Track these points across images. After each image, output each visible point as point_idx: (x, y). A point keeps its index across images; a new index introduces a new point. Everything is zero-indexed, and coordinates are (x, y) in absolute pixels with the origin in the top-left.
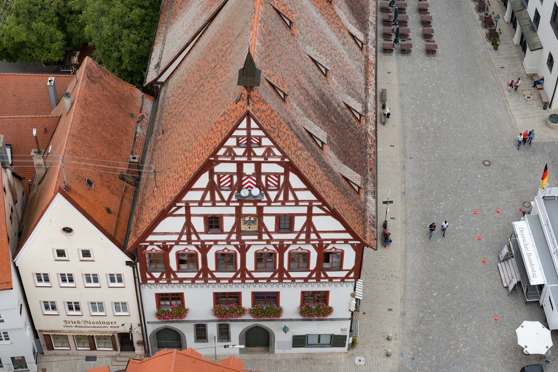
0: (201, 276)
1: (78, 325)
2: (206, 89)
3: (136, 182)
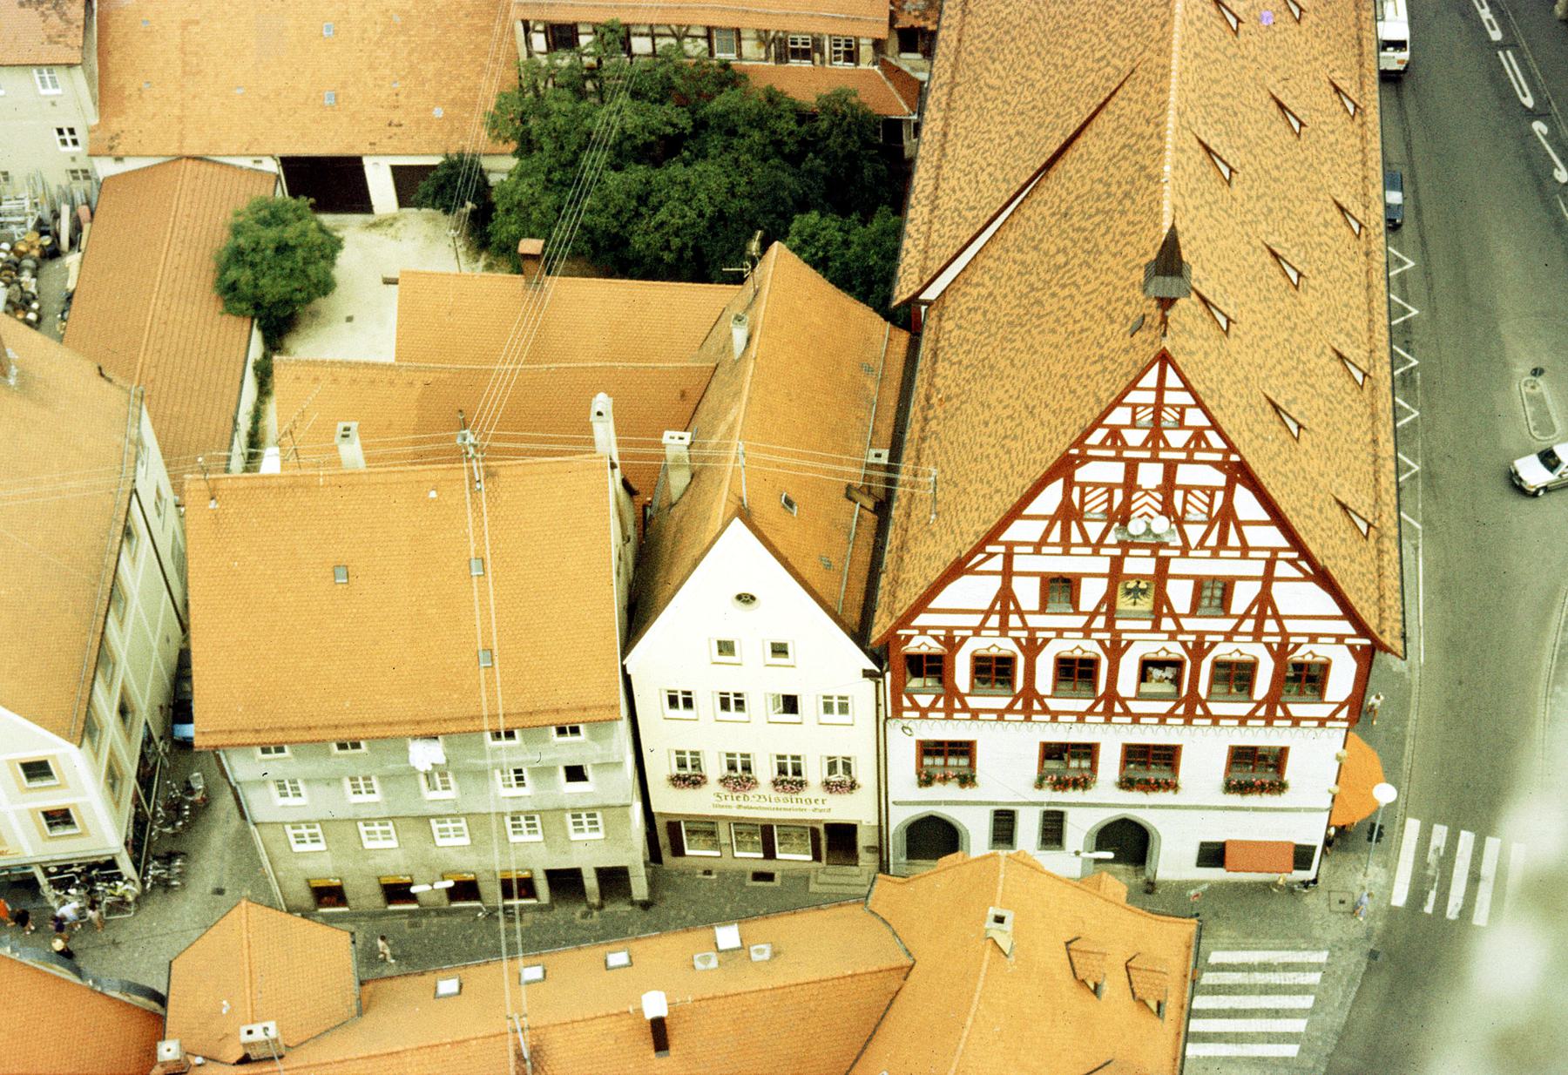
0: (1019, 706)
1: (745, 804)
2: (1049, 309)
3: (883, 508)
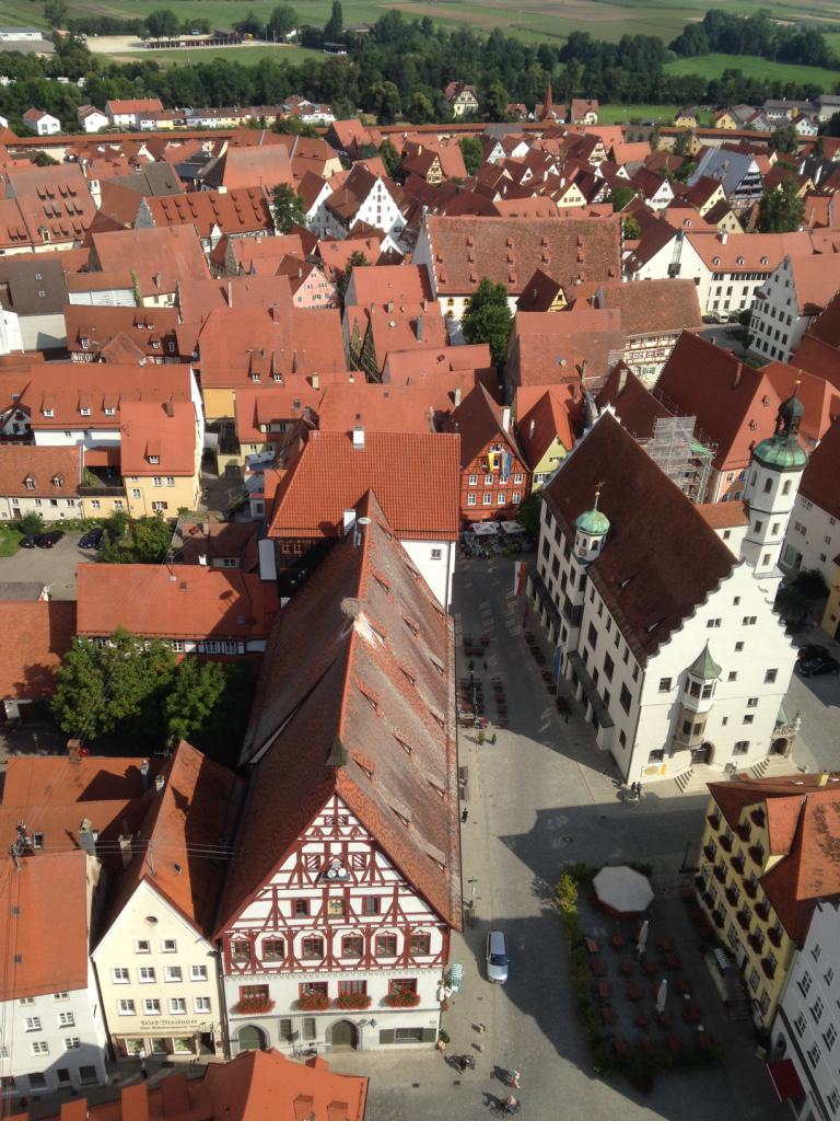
0: (287, 965)
